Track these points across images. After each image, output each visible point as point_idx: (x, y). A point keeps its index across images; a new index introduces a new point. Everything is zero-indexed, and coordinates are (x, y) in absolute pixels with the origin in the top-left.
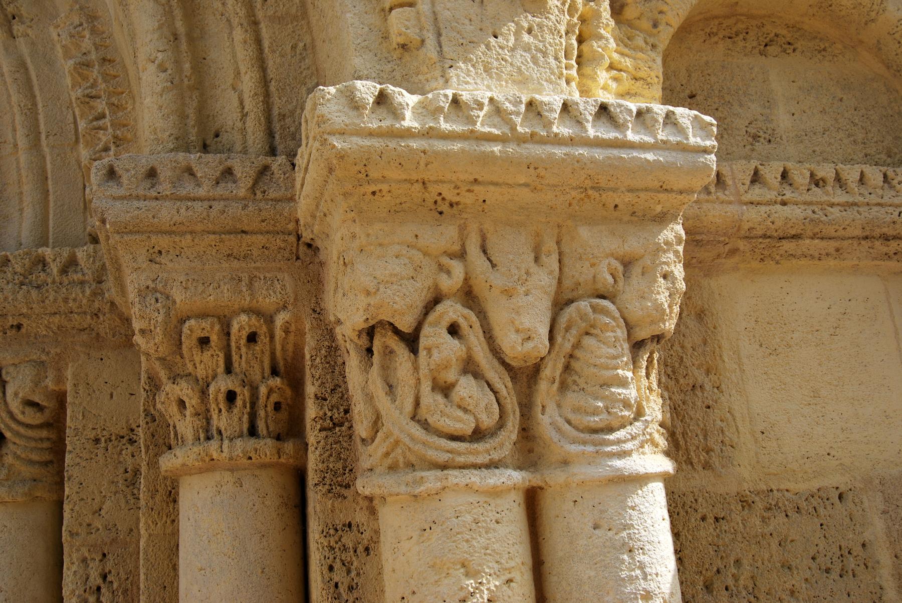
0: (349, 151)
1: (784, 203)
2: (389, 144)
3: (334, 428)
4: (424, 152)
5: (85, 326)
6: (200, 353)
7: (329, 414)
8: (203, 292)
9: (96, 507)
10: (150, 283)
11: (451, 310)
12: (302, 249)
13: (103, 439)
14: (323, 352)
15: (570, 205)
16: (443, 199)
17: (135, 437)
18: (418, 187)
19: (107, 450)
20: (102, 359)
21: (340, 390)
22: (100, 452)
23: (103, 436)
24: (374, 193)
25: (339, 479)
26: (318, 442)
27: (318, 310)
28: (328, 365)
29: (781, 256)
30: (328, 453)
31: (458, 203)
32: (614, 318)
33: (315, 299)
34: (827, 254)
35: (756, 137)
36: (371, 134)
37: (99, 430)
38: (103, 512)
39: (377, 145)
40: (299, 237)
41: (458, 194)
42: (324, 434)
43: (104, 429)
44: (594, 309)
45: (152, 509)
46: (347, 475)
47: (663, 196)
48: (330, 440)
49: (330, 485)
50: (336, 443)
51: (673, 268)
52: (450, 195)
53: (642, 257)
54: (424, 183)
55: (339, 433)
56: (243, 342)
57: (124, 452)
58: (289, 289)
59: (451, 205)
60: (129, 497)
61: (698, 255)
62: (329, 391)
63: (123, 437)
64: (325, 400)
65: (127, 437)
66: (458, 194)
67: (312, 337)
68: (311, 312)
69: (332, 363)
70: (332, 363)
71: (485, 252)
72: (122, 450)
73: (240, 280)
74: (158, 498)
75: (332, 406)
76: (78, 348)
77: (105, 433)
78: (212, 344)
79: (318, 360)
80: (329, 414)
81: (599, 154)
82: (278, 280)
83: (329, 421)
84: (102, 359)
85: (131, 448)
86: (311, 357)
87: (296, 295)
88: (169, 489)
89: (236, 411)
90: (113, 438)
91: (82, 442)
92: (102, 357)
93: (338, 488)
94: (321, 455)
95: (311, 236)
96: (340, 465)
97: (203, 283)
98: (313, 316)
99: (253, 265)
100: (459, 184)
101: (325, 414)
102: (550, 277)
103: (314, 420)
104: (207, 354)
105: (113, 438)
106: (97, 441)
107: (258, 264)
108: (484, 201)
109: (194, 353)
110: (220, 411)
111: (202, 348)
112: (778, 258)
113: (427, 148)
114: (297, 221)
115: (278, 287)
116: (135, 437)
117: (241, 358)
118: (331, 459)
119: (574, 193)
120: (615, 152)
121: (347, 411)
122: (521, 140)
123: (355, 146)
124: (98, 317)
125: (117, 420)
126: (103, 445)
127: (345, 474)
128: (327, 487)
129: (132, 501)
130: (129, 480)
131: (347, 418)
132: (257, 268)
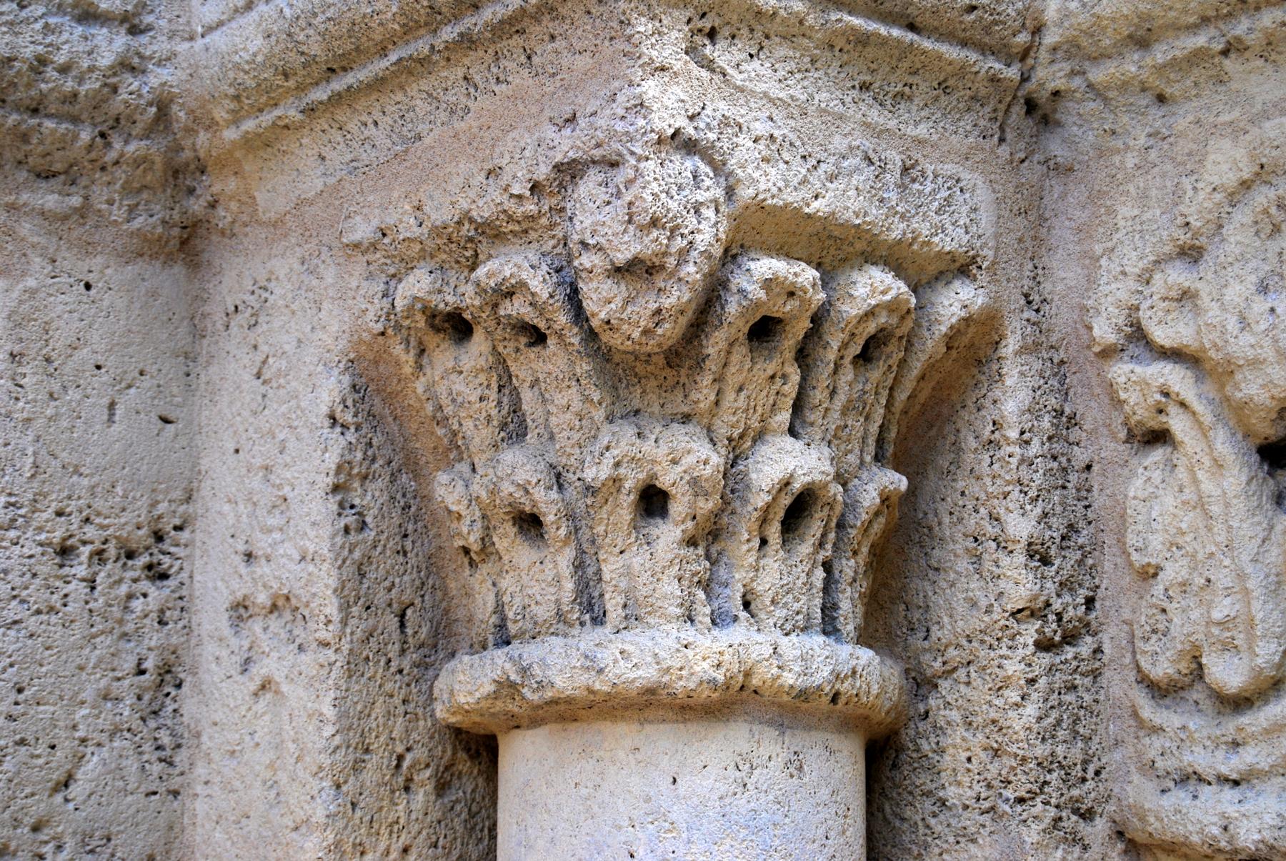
3: (1060, 645)
5: (58, 167)
6: (748, 365)
7: (1057, 605)
8: (804, 181)
9: (58, 776)
10: (681, 122)
12: (1018, 110)
13: (85, 551)
14: (1046, 423)
17: (166, 560)
19: (93, 588)
20: (88, 286)
21: (1080, 541)
22: (77, 589)
23: (84, 543)
25: (1075, 792)
26: (1032, 682)
27: (1035, 297)
28: (1055, 465)
30: (1054, 714)
33: (1030, 266)
37: (76, 520)
38: (75, 790)
40: (1025, 79)
42: (1046, 659)
43: (87, 520)
45: (354, 805)
46: (1090, 784)
48: (1060, 679)
49: (1057, 807)
50: (1069, 689)
55: (1075, 663)
57: (137, 604)
58: (986, 220)
60: (149, 753)
62: (1058, 540)
63: (130, 555)
64: (1046, 561)
65: (144, 560)
67: (1022, 374)
68: (1023, 302)
69: (1063, 460)
70: (1063, 460)
72: (130, 597)
74: (369, 776)
75: (1061, 584)
76: (25, 228)
77: (90, 532)
79: (1035, 448)
80: (1057, 605)
82: (962, 191)
83: (1054, 626)
84: (88, 286)
85: (157, 595)
86: (1022, 433)
87: (997, 249)
88: (400, 749)
89: (805, 548)
90: (112, 551)
91: (26, 551)
92: (91, 278)
93: (1074, 818)
94: (1040, 719)
95: (1060, 83)
96: (1076, 753)
97: (803, 157)
98: (1026, 315)
101: (1048, 605)
103: (1013, 614)
105: (112, 551)
106: (65, 552)
109: (735, 358)
110: (764, 542)
111: (751, 351)
114: (1038, 30)
115: (965, 209)
116: (166, 560)
118: (1061, 734)
121: (1090, 602)
124: (108, 145)
125: (125, 496)
126: (81, 571)
127: (1084, 780)
128: (1052, 812)
129: (157, 768)
130: (147, 697)
131: (1088, 625)
132: (920, 142)
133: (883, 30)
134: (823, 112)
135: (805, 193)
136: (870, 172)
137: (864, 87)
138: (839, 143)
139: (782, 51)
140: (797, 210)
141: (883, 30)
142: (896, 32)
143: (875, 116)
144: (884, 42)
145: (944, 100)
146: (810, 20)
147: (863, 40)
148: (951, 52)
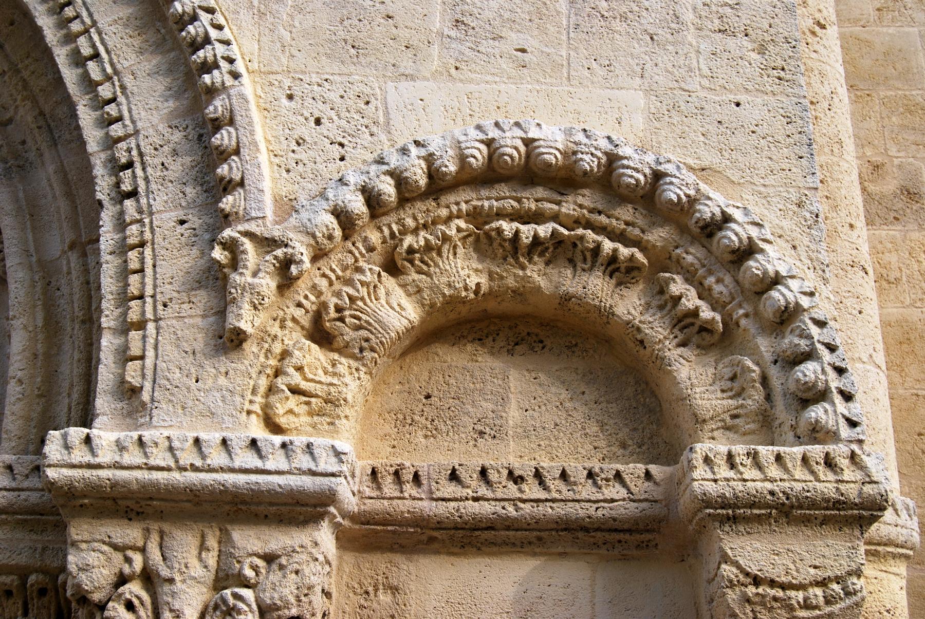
0: (57, 480)
1: (476, 499)
2: (85, 474)
4: (109, 479)
8: (10, 557)
11: (134, 589)
15: (228, 514)
16: (132, 510)
18: (109, 503)
24: (81, 506)
29: (482, 543)
31: (143, 513)
32: (249, 606)
34: (530, 543)
35: (482, 433)
36: (73, 466)
39: (76, 475)
41: (141, 507)
44: (237, 596)
47: (299, 509)
51: (305, 567)
52: (136, 508)
53: (279, 556)
54: (114, 500)
56: (35, 594)
59: (138, 513)
61: (399, 541)
66: (141, 507)
71: (161, 548)
73: (35, 550)
78: (14, 595)
81: (241, 479)
99: (47, 538)
100: (139, 501)
102: (204, 570)
104: (11, 601)
107: (50, 538)
108: (162, 512)
112: (479, 545)
113: (111, 476)
117: (34, 606)
119: (227, 507)
120: (253, 478)
122: (183, 469)
123: (61, 476)
132: (49, 541)
133: (29, 517)
134: (17, 539)
135: (10, 559)
136: (31, 551)
137: (31, 531)
138: (22, 546)
139: (4, 527)
140: (7, 565)
141: (29, 517)
142: (32, 517)
143: (34, 537)
144: (31, 520)
145: (57, 529)
146: (9, 519)
147: (25, 520)
148: (51, 518)
